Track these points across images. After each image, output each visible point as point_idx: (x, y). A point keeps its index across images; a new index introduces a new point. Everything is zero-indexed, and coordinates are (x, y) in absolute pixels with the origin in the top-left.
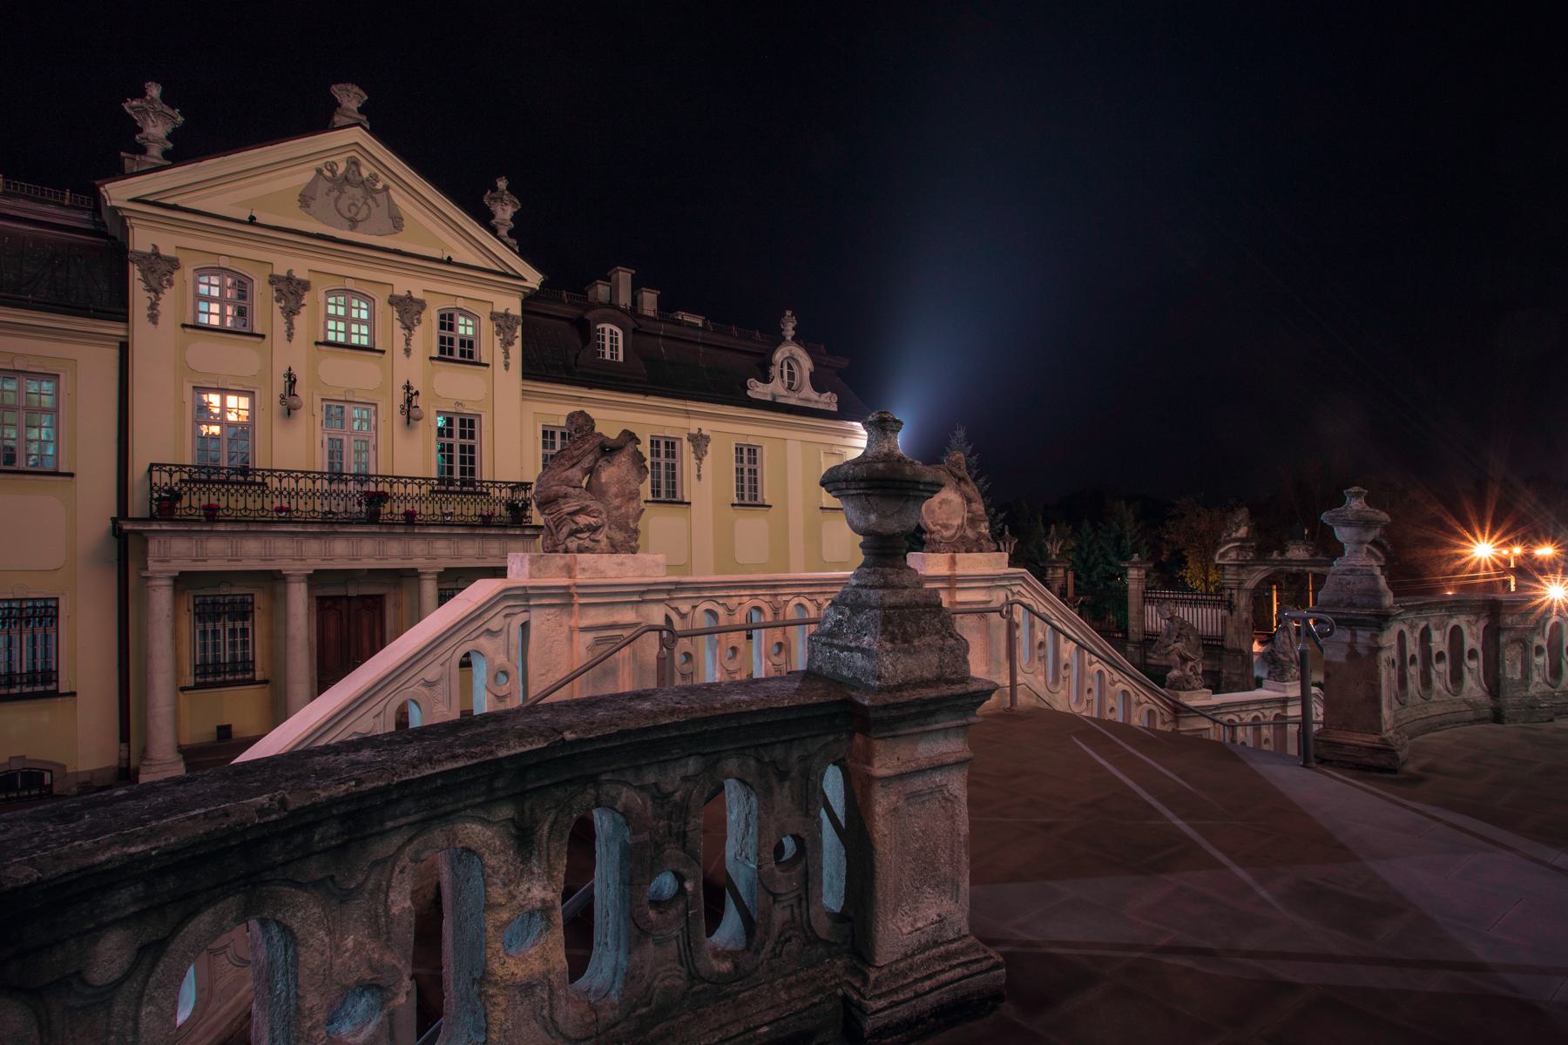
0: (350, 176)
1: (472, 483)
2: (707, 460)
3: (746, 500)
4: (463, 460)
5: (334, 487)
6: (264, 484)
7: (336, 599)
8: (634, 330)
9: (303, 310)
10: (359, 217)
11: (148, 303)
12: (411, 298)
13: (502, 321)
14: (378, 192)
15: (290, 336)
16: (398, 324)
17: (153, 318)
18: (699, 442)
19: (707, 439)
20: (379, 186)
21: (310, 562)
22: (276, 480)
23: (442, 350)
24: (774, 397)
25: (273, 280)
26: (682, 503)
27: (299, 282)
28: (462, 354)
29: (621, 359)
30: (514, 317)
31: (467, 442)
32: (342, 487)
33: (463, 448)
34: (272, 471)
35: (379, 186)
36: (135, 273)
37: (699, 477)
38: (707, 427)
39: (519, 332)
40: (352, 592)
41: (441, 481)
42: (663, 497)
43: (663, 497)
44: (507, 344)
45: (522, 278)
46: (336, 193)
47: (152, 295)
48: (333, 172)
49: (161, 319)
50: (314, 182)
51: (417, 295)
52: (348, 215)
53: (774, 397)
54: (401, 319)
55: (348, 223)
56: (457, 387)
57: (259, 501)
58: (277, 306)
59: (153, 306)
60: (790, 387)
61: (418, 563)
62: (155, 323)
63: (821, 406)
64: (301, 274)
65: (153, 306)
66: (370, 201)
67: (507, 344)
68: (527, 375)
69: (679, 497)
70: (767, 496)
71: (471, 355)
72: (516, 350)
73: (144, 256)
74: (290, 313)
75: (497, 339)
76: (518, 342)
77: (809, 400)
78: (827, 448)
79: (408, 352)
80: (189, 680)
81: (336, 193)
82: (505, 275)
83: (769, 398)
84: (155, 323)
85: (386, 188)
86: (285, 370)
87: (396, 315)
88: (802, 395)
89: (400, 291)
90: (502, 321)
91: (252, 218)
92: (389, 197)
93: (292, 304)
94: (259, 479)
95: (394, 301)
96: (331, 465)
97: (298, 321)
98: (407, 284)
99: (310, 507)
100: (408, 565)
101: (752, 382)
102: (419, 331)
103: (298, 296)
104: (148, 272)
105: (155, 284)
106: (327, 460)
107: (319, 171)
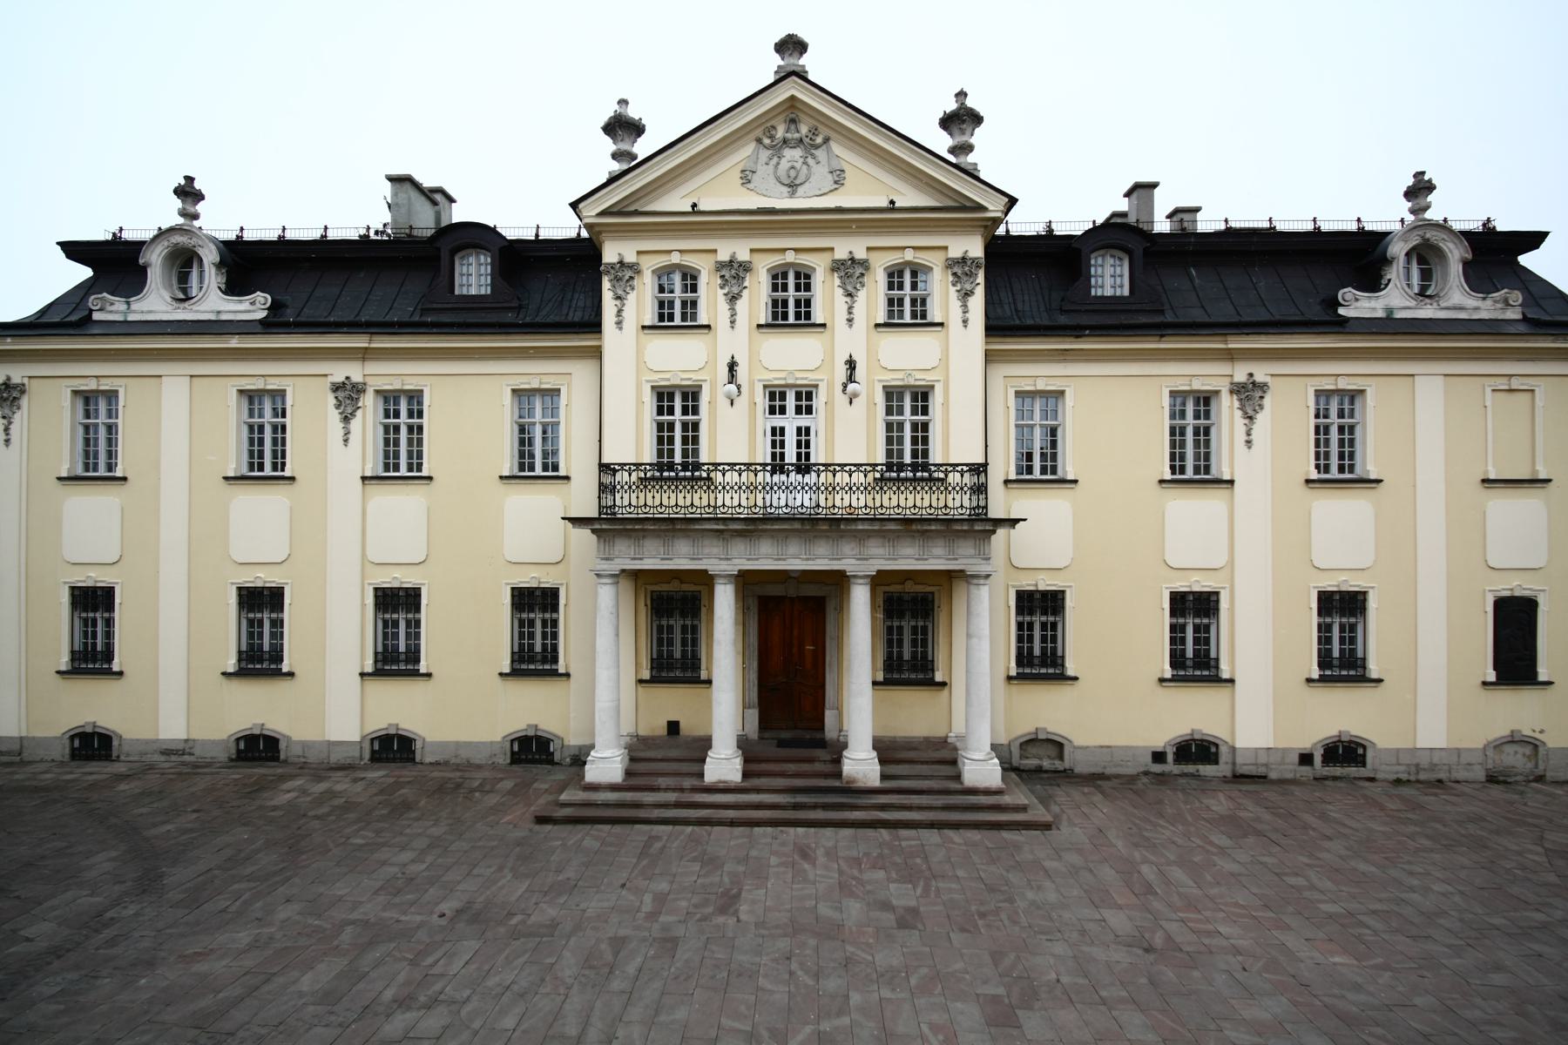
0: (789, 135)
1: (925, 467)
2: (1262, 419)
3: (1334, 473)
4: (914, 441)
5: (776, 478)
6: (709, 478)
7: (779, 600)
8: (1146, 252)
9: (745, 293)
12: (852, 259)
13: (960, 268)
14: (817, 147)
15: (733, 322)
17: (619, 324)
18: (1250, 394)
19: (1263, 387)
20: (819, 140)
21: (736, 561)
22: (719, 474)
23: (891, 314)
24: (1390, 311)
25: (720, 266)
26: (1219, 481)
27: (740, 264)
29: (1126, 292)
30: (973, 260)
32: (784, 477)
34: (716, 465)
35: (819, 140)
36: (606, 284)
37: (1249, 442)
38: (1262, 372)
39: (981, 278)
40: (792, 593)
41: (889, 467)
42: (1189, 474)
43: (1189, 474)
44: (966, 295)
45: (983, 208)
46: (776, 159)
48: (772, 137)
51: (860, 254)
53: (1390, 311)
54: (843, 286)
55: (785, 189)
56: (907, 355)
57: (705, 496)
58: (721, 292)
59: (620, 311)
60: (1422, 293)
61: (848, 564)
63: (1484, 315)
64: (744, 256)
65: (620, 311)
66: (810, 160)
68: (994, 329)
69: (1214, 473)
70: (1370, 463)
72: (977, 302)
73: (612, 266)
74: (733, 299)
75: (952, 290)
76: (980, 292)
77: (1461, 309)
78: (1502, 384)
81: (776, 159)
83: (1380, 314)
85: (826, 140)
86: (728, 360)
87: (837, 282)
88: (1443, 305)
89: (841, 254)
90: (960, 268)
91: (694, 205)
92: (829, 150)
93: (735, 290)
94: (704, 475)
96: (889, 453)
97: (741, 305)
98: (844, 247)
99: (736, 503)
101: (1346, 293)
102: (862, 295)
103: (739, 278)
104: (617, 279)
105: (620, 292)
106: (769, 450)
107: (759, 141)
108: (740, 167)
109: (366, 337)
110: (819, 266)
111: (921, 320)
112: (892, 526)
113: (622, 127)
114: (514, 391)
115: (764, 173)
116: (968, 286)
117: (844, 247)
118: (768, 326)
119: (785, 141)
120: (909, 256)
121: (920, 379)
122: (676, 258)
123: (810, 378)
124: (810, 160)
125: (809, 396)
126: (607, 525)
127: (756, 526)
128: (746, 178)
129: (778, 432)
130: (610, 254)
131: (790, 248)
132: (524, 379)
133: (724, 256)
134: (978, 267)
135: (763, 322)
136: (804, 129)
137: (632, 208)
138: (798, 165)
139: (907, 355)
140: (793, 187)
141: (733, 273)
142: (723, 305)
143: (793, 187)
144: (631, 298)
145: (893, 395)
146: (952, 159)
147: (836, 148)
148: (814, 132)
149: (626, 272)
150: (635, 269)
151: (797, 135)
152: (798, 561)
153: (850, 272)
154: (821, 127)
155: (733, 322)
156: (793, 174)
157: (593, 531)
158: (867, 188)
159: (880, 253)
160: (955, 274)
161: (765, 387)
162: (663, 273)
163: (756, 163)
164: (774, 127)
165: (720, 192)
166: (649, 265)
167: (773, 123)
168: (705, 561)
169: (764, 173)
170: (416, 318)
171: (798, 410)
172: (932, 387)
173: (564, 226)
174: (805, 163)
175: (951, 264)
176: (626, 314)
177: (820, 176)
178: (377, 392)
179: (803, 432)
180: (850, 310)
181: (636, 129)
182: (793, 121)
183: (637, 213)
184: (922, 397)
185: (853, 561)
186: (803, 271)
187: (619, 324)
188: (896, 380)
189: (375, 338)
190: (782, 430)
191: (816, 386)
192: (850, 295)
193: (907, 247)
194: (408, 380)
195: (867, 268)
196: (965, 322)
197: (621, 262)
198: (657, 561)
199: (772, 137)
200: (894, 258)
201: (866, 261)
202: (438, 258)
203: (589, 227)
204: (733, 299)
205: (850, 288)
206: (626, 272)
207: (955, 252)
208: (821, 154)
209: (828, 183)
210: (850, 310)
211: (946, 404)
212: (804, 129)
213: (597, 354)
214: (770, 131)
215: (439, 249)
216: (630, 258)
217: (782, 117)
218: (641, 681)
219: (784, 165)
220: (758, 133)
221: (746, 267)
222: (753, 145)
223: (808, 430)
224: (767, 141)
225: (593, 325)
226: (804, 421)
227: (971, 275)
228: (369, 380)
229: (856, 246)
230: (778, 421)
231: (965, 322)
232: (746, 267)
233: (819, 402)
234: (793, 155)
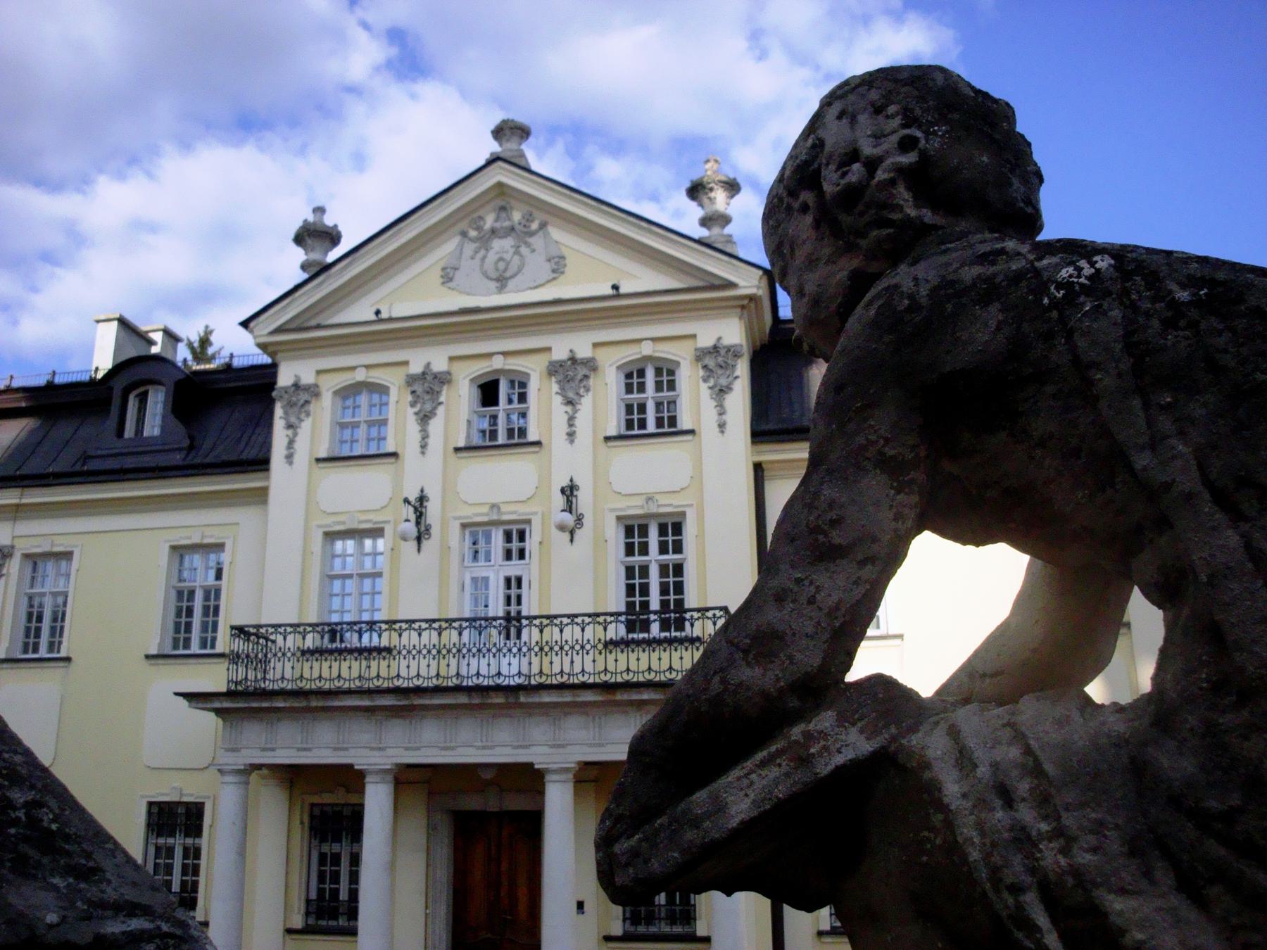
0: (498, 225)
7: (481, 817)
9: (441, 410)
10: (508, 274)
11: (286, 441)
12: (573, 360)
13: (714, 360)
14: (532, 234)
15: (424, 447)
16: (558, 400)
17: (289, 458)
20: (534, 226)
21: (390, 752)
23: (629, 424)
25: (411, 380)
27: (435, 376)
28: (660, 422)
31: (671, 557)
33: (664, 570)
35: (534, 226)
36: (279, 411)
44: (721, 392)
45: (731, 285)
47: (290, 432)
49: (296, 458)
50: (461, 248)
51: (584, 352)
52: (494, 275)
54: (562, 392)
55: (493, 285)
56: (650, 474)
58: (411, 411)
61: (538, 756)
62: (291, 463)
64: (440, 363)
66: (524, 250)
67: (721, 392)
68: (759, 436)
71: (673, 421)
72: (739, 401)
73: (286, 390)
74: (424, 418)
79: (571, 435)
80: (298, 922)
81: (483, 252)
82: (712, 287)
84: (291, 463)
85: (543, 226)
87: (555, 388)
89: (560, 353)
90: (714, 360)
91: (378, 312)
92: (547, 235)
93: (428, 407)
95: (555, 369)
97: (436, 426)
98: (563, 345)
100: (521, 757)
102: (586, 403)
103: (433, 393)
104: (291, 405)
107: (464, 234)
108: (442, 264)
109: (17, 492)
110: (534, 368)
111: (669, 426)
112: (589, 696)
113: (315, 235)
114: (174, 548)
115: (469, 268)
116: (723, 381)
117: (563, 345)
118: (469, 448)
119: (493, 231)
120: (647, 349)
121: (667, 505)
122: (360, 375)
123: (520, 512)
124: (524, 250)
125: (522, 536)
126: (241, 704)
127: (408, 702)
128: (448, 277)
129: (481, 583)
130: (285, 378)
131: (495, 352)
132: (184, 533)
133: (416, 368)
134: (737, 355)
135: (461, 444)
136: (517, 216)
137: (313, 323)
138: (507, 257)
139: (650, 474)
140: (502, 282)
141: (428, 388)
142: (413, 427)
143: (502, 282)
144: (306, 426)
145: (634, 531)
146: (702, 233)
147: (556, 233)
148: (529, 218)
149: (304, 394)
150: (313, 391)
151: (507, 224)
152: (471, 751)
153: (573, 375)
154: (536, 213)
155: (424, 447)
156: (501, 265)
157: (218, 712)
158: (591, 273)
159: (610, 351)
160: (705, 367)
161: (464, 526)
162: (348, 393)
163: (460, 258)
164: (481, 218)
165: (416, 293)
166: (329, 384)
167: (481, 213)
168: (352, 752)
169: (469, 268)
170: (78, 468)
171: (508, 555)
172: (683, 514)
173: (237, 346)
174: (517, 252)
175: (701, 355)
176: (296, 443)
177: (536, 264)
178: (27, 556)
179: (514, 583)
180: (571, 421)
181: (332, 237)
182: (503, 208)
183: (318, 327)
184: (672, 529)
185: (545, 749)
186: (517, 379)
187: (289, 458)
188: (635, 507)
189: (28, 491)
190: (486, 579)
191: (529, 522)
192: (570, 402)
193: (644, 339)
194: (59, 540)
195: (595, 369)
196: (722, 426)
197: (296, 386)
198: (293, 752)
199: (479, 229)
200: (629, 354)
201: (592, 360)
202: (108, 401)
203: (263, 347)
204: (424, 418)
205: (571, 395)
206: (304, 394)
207: (706, 341)
208: (536, 241)
209: (545, 270)
210: (571, 421)
211: (701, 536)
212: (517, 216)
213: (261, 496)
214: (477, 223)
215: (111, 389)
216: (308, 378)
217: (492, 204)
218: (289, 931)
219: (492, 257)
220: (463, 225)
221: (443, 379)
222: (456, 240)
223: (519, 580)
224: (473, 233)
225: (261, 464)
226: (514, 568)
227: (727, 367)
228: (17, 546)
229: (580, 343)
230: (481, 570)
231: (722, 426)
232: (443, 379)
233: (531, 544)
234: (502, 245)
